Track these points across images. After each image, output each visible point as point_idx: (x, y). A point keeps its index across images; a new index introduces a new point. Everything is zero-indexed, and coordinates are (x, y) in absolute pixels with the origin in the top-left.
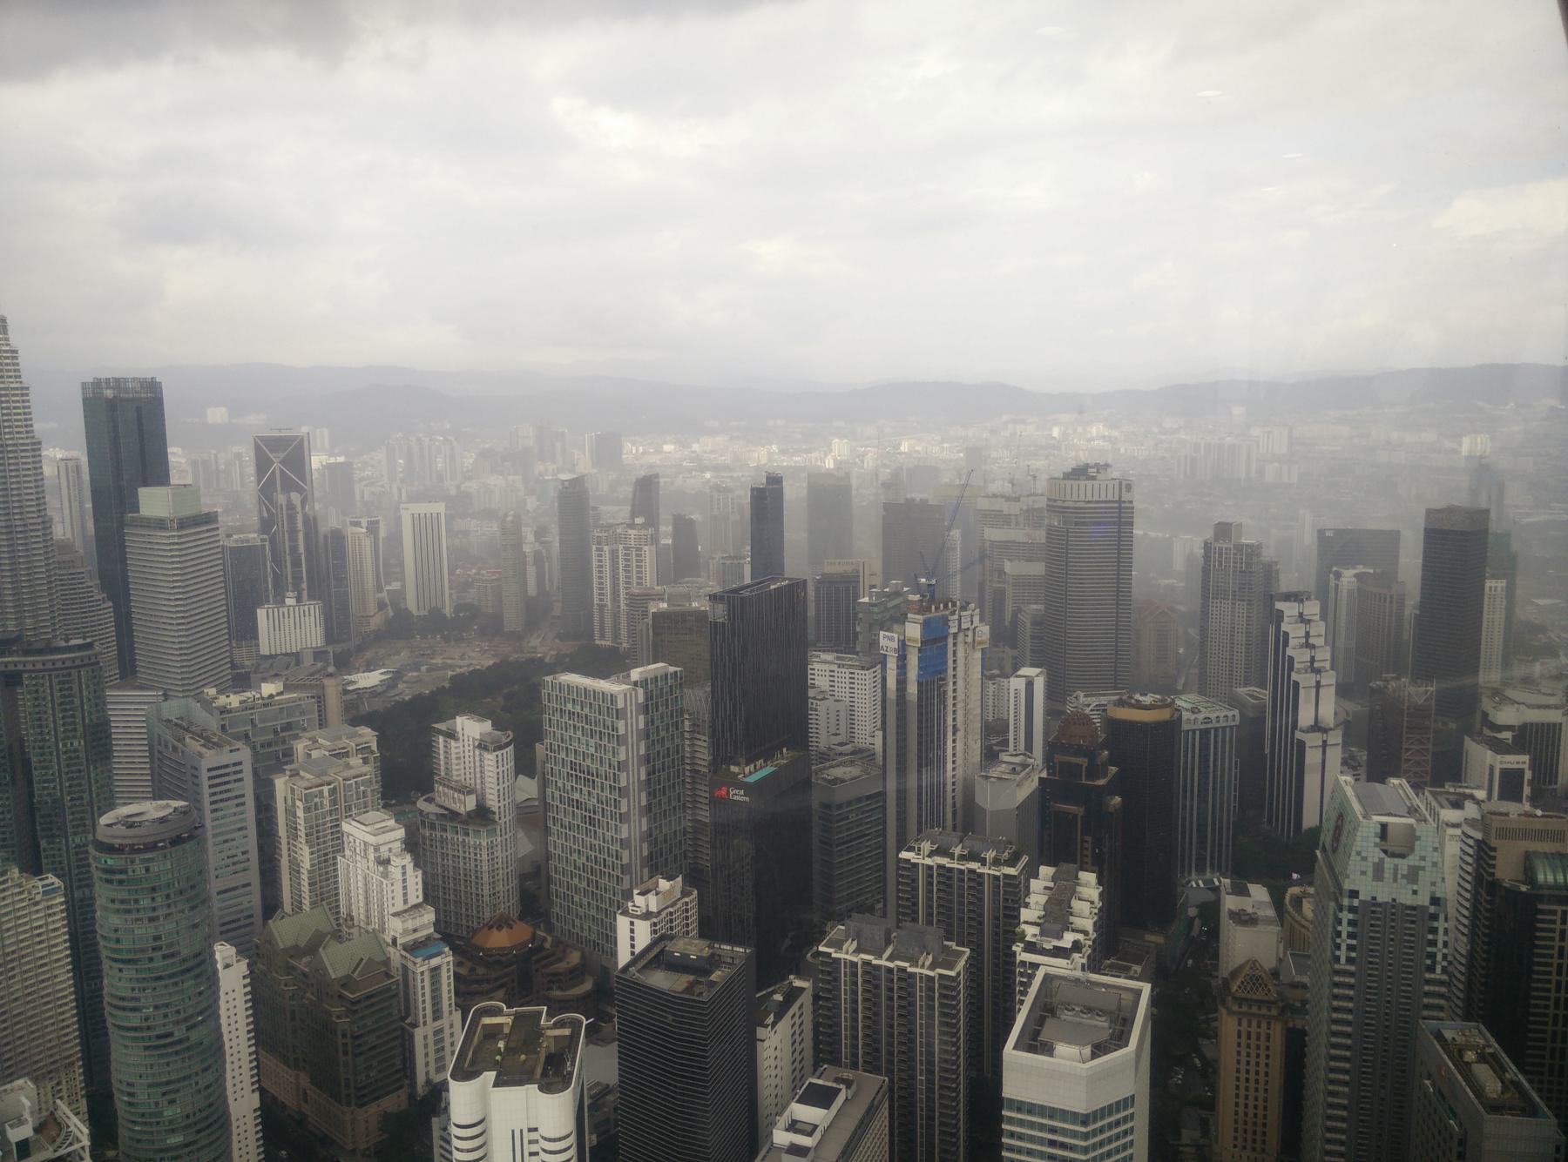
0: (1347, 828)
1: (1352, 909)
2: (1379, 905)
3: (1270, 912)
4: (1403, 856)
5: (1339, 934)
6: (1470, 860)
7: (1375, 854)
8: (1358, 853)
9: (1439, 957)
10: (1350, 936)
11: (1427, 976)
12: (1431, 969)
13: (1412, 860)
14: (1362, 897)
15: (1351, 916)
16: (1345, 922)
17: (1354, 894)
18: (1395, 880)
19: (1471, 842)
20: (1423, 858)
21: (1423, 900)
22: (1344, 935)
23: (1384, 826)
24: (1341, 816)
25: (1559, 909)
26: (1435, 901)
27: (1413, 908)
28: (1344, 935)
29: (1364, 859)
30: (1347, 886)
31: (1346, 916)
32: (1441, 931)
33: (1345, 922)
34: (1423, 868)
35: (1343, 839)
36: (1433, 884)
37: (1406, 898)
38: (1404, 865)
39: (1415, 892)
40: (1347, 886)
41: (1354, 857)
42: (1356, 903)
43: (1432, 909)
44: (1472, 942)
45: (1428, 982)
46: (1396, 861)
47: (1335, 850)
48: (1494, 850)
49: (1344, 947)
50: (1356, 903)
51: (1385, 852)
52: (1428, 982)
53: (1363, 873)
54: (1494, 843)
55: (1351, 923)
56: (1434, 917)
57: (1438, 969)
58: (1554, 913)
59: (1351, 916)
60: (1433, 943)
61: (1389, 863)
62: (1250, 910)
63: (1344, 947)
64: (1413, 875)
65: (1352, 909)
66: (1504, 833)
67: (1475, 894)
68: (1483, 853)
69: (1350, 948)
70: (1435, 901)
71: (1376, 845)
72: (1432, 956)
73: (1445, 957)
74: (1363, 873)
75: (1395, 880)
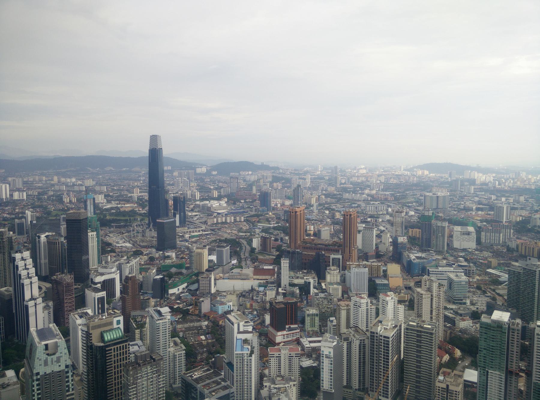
0: (33, 349)
1: (37, 380)
2: (48, 375)
3: (15, 380)
4: (54, 354)
5: (34, 391)
6: (84, 339)
7: (44, 357)
8: (38, 358)
9: (70, 386)
10: (38, 390)
11: (67, 394)
12: (68, 391)
13: (58, 355)
14: (41, 374)
15: (37, 382)
16: (35, 385)
17: (38, 374)
18: (52, 364)
19: (84, 333)
20: (61, 353)
21: (63, 367)
22: (36, 390)
23: (46, 345)
24: (31, 345)
25: (113, 348)
26: (67, 366)
27: (60, 372)
28: (36, 390)
29: (40, 360)
30: (35, 372)
31: (35, 383)
32: (70, 376)
33: (35, 385)
34: (62, 356)
35: (33, 353)
36: (66, 361)
37: (56, 369)
38: (54, 357)
39: (60, 366)
40: (35, 372)
41: (36, 360)
42: (39, 377)
43: (66, 370)
44: (88, 367)
45: (68, 396)
46: (52, 357)
47: (30, 358)
48: (91, 334)
49: (36, 395)
50: (39, 377)
51: (48, 354)
52: (68, 396)
53: (40, 365)
54: (91, 332)
55: (38, 385)
56: (67, 372)
57: (71, 390)
58: (111, 350)
59: (37, 382)
60: (68, 382)
61: (49, 358)
62: (7, 382)
63: (36, 395)
64: (58, 360)
65: (37, 380)
66: (95, 327)
67: (87, 350)
68: (88, 335)
69: (38, 394)
70: (67, 366)
71: (44, 353)
72: (68, 386)
73: (72, 385)
74: (40, 365)
75: (52, 364)
